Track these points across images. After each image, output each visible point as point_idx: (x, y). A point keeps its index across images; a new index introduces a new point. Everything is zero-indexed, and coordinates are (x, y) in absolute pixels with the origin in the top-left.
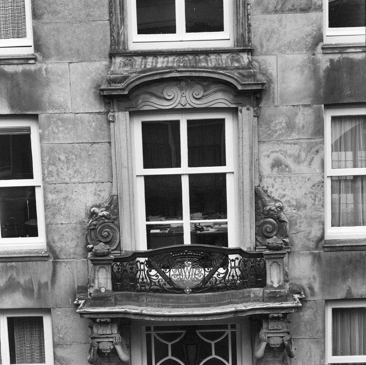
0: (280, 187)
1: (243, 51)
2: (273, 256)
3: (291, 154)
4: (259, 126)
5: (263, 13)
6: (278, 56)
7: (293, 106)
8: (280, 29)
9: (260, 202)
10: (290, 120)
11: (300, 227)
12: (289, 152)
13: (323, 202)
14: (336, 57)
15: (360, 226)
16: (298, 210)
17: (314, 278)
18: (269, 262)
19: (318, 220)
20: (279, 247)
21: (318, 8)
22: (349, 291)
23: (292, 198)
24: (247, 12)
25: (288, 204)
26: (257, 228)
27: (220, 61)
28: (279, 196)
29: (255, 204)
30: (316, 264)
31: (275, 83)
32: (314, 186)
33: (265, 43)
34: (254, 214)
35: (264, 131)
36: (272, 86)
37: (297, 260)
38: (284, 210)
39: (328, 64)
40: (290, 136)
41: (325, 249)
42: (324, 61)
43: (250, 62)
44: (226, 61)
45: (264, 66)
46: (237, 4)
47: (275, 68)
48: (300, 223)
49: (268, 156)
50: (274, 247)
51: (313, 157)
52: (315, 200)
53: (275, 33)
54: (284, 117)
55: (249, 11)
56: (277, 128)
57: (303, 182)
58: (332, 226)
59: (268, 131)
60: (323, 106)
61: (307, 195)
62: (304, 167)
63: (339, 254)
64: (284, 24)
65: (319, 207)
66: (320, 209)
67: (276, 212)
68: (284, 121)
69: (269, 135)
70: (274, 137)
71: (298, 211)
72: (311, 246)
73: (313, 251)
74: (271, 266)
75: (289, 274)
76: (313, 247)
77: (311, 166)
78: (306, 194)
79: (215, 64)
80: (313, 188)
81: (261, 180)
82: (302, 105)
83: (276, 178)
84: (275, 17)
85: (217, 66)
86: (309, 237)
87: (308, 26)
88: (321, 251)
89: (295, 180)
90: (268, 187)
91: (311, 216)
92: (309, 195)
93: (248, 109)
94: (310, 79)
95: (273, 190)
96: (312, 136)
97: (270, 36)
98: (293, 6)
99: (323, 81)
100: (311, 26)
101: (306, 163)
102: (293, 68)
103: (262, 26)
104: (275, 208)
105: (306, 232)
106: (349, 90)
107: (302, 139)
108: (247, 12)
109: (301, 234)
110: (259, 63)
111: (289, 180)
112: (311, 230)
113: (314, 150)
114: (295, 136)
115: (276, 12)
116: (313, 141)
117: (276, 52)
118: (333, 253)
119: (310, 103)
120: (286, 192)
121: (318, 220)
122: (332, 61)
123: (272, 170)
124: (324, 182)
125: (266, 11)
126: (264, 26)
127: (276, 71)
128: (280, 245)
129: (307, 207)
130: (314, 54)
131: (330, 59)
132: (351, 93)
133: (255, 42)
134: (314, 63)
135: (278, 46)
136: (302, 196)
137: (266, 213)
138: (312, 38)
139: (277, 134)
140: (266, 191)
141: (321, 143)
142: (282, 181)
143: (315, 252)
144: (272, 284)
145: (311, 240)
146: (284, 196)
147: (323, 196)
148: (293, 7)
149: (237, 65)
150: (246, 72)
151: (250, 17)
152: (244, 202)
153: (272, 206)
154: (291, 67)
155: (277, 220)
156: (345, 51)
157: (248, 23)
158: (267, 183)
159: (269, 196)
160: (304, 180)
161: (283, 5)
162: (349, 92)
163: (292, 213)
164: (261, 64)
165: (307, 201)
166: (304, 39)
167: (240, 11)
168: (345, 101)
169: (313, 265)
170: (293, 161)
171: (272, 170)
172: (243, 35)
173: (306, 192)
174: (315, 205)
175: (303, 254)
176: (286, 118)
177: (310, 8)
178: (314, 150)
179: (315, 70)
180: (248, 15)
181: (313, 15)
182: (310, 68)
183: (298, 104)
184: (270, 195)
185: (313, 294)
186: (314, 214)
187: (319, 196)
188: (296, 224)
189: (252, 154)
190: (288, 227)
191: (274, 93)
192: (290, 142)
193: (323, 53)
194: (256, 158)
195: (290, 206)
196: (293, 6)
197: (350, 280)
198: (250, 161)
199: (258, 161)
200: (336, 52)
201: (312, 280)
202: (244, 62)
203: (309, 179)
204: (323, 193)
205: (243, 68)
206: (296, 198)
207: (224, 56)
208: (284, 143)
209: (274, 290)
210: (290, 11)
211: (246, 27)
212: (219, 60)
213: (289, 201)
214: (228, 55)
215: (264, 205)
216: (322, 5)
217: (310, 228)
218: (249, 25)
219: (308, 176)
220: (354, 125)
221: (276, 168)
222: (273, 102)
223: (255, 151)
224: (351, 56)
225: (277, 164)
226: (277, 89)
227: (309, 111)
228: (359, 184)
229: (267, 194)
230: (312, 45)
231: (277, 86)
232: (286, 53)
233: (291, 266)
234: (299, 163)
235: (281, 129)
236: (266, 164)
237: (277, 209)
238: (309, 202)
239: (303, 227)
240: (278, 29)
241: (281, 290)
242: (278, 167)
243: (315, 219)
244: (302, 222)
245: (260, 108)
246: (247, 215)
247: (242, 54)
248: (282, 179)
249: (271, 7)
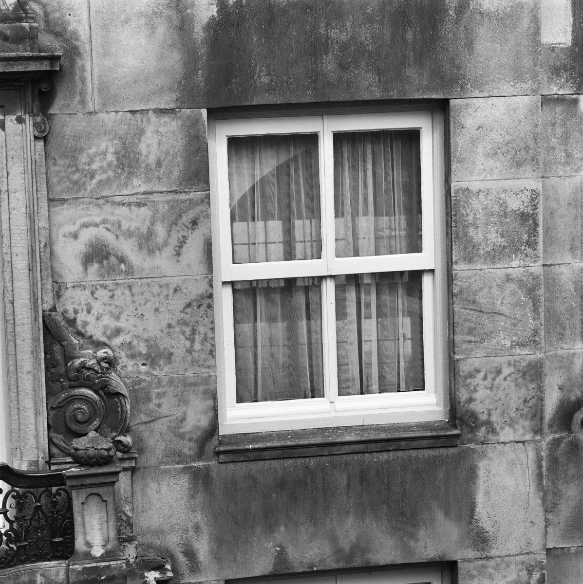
0: (107, 311)
2: (88, 481)
3: (132, 229)
4: (51, 162)
7: (133, 112)
9: (57, 348)
10: (125, 148)
11: (159, 405)
12: (125, 225)
13: (213, 345)
15: (305, 397)
16: (152, 365)
17: (197, 528)
18: (78, 495)
19: (202, 388)
20: (103, 457)
22: (281, 557)
23: (138, 337)
25: (129, 353)
26: (52, 413)
28: (104, 334)
29: (46, 353)
30: (199, 494)
31: (86, 55)
32: (189, 305)
34: (44, 380)
35: (62, 174)
36: (80, 63)
37: (153, 486)
38: (119, 368)
39: (214, 11)
40: (126, 185)
41: (221, 456)
45: (57, 15)
47: (85, 21)
48: (159, 396)
49: (75, 236)
50: (90, 458)
51: (184, 237)
52: (192, 340)
54: (111, 140)
56: (95, 166)
57: (162, 296)
58: (240, 400)
59: (74, 173)
60: (204, 112)
61: (174, 327)
62: (163, 261)
63: (254, 467)
65: (203, 356)
66: (205, 360)
67: (97, 372)
68: (111, 150)
69: (76, 183)
70: (89, 188)
71: (154, 369)
72: (186, 451)
73: (192, 464)
74: (85, 505)
75: (134, 520)
76: (192, 453)
77: (180, 258)
78: (170, 326)
80: (188, 310)
81: (58, 296)
82: (155, 111)
83: (97, 289)
86: (182, 430)
88: (210, 463)
89: (143, 294)
90: (76, 312)
91: (184, 378)
92: (177, 329)
93: (20, 120)
95: (90, 318)
96: (180, 184)
99: (203, 51)
101: (169, 251)
102: (127, 20)
104: (94, 361)
105: (174, 417)
107: (157, 192)
109: (163, 422)
111: (127, 292)
112: (185, 414)
113: (186, 219)
114: (139, 185)
116: (183, 197)
118: (239, 465)
119: (172, 105)
120: (123, 323)
121: (202, 388)
123: (86, 269)
124: (214, 296)
127: (87, 27)
128: (106, 453)
129: (173, 358)
132: (271, 82)
136: (162, 331)
137: (72, 374)
139: (95, 181)
140: (72, 322)
141: (202, 201)
142: (112, 297)
143: (196, 465)
144: (88, 550)
145: (187, 437)
146: (117, 332)
147: (213, 329)
150: (10, 28)
152: (18, 348)
153: (87, 357)
154: (123, 17)
155: (101, 392)
158: (73, 301)
159: (79, 334)
160: (165, 292)
162: (265, 80)
163: (140, 373)
164: (49, 10)
165: (173, 342)
168: (258, 101)
169: (193, 496)
170: (136, 248)
171: (86, 269)
173: (170, 321)
174: (193, 353)
175: (168, 471)
176: (116, 141)
178: (186, 219)
179: (183, 25)
182: (169, 18)
183: (144, 108)
184: (83, 331)
185: (195, 566)
186: (192, 373)
187: (202, 329)
188: (149, 400)
189: (32, 231)
190: (128, 407)
191: (83, 80)
192: (127, 200)
194: (43, 240)
195: (132, 357)
197: (283, 529)
198: (30, 248)
199: (48, 248)
201: (191, 533)
203: (176, 290)
204: (212, 322)
206: (145, 336)
208: (114, 203)
209: (94, 565)
213: (130, 343)
215: (69, 356)
217: (182, 409)
219: (175, 282)
220: (283, 159)
221: (96, 266)
222: (83, 102)
223: (42, 223)
225: (97, 254)
226: (92, 69)
227: (171, 125)
228: (300, 299)
229: (75, 328)
231: (92, 63)
233: (138, 503)
234: (151, 251)
235: (103, 170)
236: (69, 255)
237: (99, 364)
238: (179, 345)
239: (167, 406)
241: (111, 563)
242: (100, 262)
243: (195, 384)
244: (164, 394)
245: (49, 117)
246: (27, 383)
248: (110, 291)
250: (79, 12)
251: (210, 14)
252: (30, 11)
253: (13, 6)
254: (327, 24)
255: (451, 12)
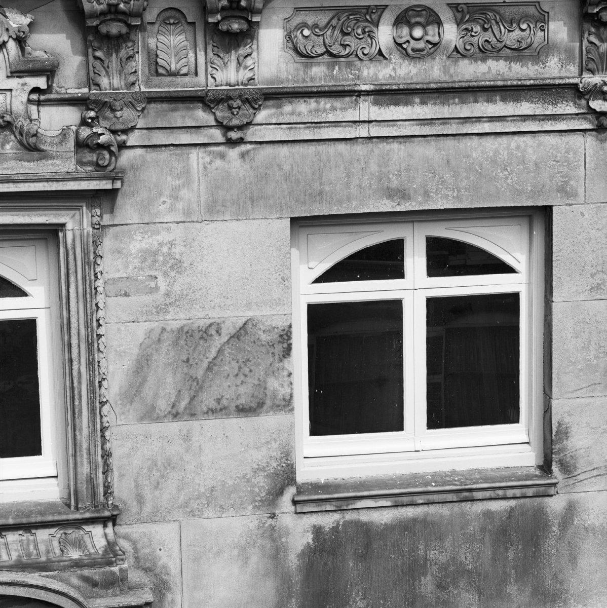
1: (92, 521)
5: (141, 419)
6: (183, 524)
8: (187, 457)
14: (328, 521)
21: (283, 403)
24: (102, 423)
27: (32, 547)
31: (176, 589)
33: (147, 493)
39: (309, 538)
42: (299, 531)
43: (111, 546)
44: (47, 547)
45: (147, 551)
46: (74, 405)
53: (174, 468)
55: (105, 419)
64: (197, 444)
79: (20, 556)
84: (174, 428)
85: (24, 559)
87: (258, 448)
94: (263, 576)
97: (162, 476)
98: (219, 401)
99: (297, 578)
100: (264, 449)
102: (220, 552)
103: (139, 453)
106: (361, 600)
108: (102, 423)
110: (134, 542)
115: (176, 416)
117: (177, 515)
122: (318, 531)
125: (150, 415)
126: (146, 451)
127: (178, 561)
130: (273, 516)
131: (315, 526)
133: (122, 490)
134: (274, 535)
135: (182, 497)
138: (268, 476)
148: (219, 403)
149: (75, 554)
150: (99, 574)
151: (107, 434)
154: (215, 550)
156: (351, 507)
157: (102, 448)
161: (193, 398)
164: (139, 546)
166: (249, 480)
167: (81, 422)
172: (91, 479)
177: (261, 405)
179: (277, 555)
180: (103, 429)
181: (269, 421)
182: (263, 548)
193: (296, 513)
196: (219, 401)
200: (328, 509)
202: (94, 546)
205: (93, 564)
207: (42, 535)
210: (210, 412)
211: (100, 458)
212: (28, 544)
214: (52, 531)
216: (291, 396)
218: (107, 455)
224: (364, 517)
230: (269, 493)
231: (182, 596)
232: (203, 516)
240: (181, 459)
247: (87, 528)
249: (163, 405)
250: (169, 547)
251: (305, 542)
252: (120, 553)
253: (103, 549)
254: (426, 545)
255: (554, 529)
